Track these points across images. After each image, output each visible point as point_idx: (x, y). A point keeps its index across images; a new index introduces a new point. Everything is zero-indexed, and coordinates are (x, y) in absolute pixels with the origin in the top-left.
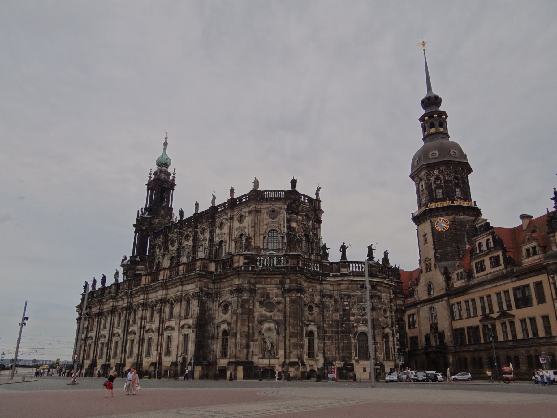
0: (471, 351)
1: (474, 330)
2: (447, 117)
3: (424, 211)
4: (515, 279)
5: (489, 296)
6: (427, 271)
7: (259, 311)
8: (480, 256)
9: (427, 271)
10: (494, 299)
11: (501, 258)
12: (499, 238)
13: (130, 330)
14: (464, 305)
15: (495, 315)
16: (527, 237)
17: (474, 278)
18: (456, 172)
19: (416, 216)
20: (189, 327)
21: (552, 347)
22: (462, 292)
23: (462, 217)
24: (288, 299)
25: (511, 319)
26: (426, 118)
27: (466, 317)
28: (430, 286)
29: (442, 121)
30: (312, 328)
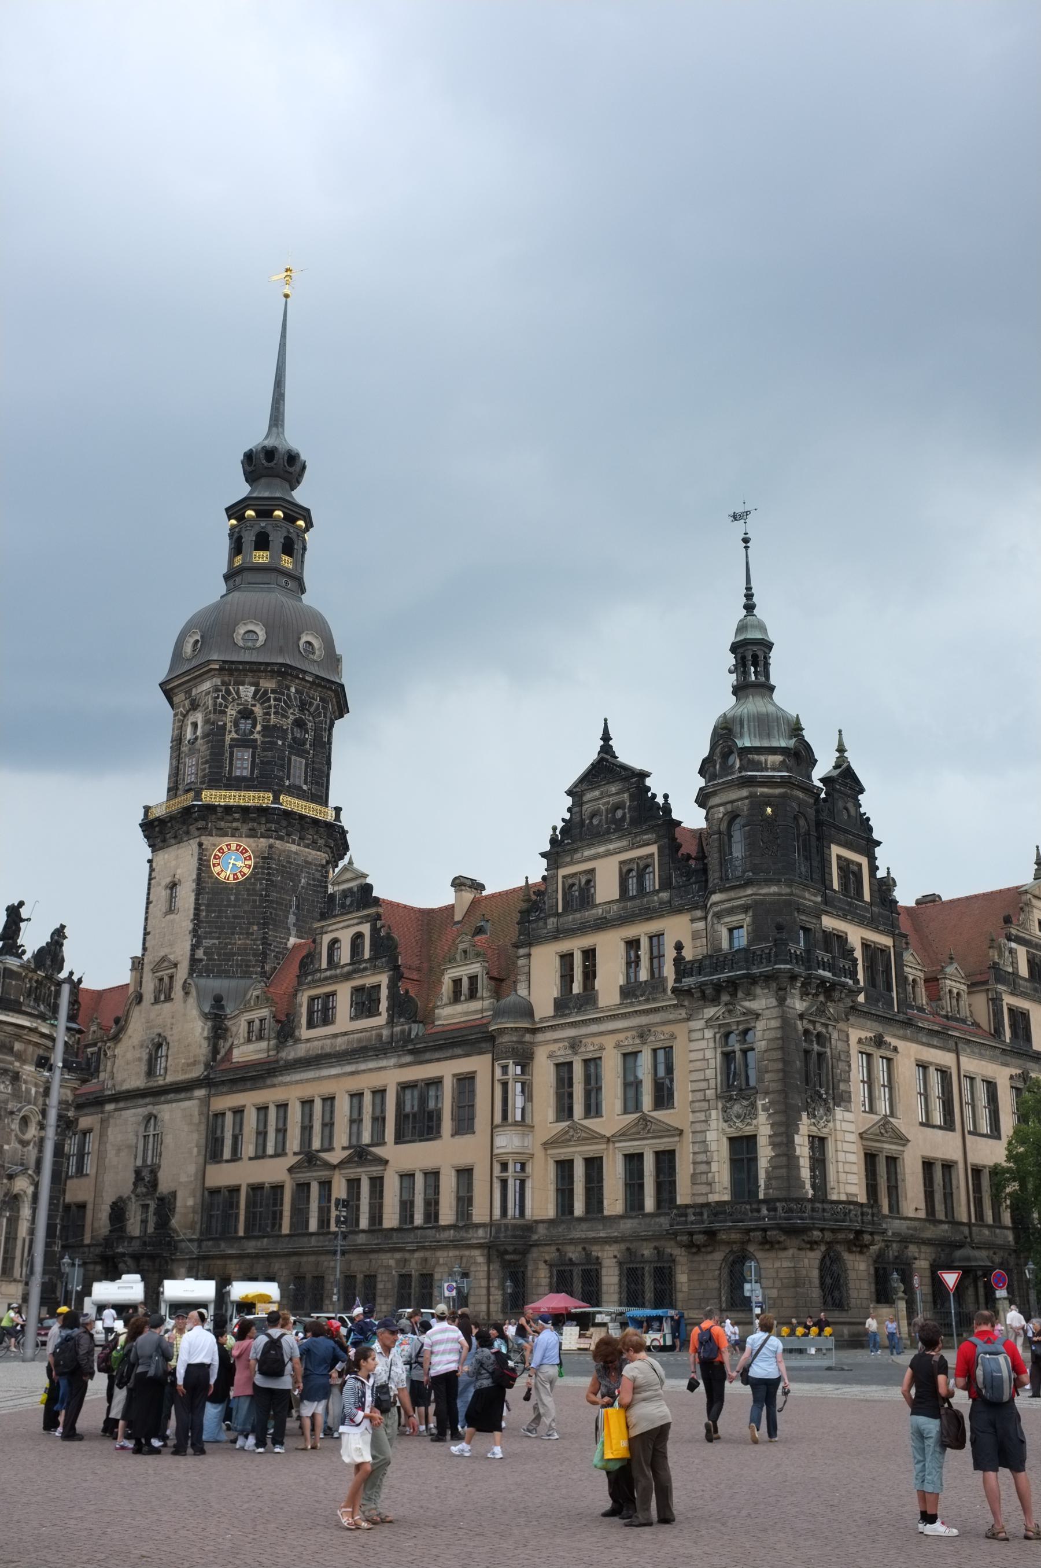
0: (249, 1256)
1: (266, 1196)
2: (309, 525)
3: (187, 810)
4: (408, 1059)
5: (329, 1100)
6: (157, 1001)
8: (326, 978)
9: (157, 1001)
10: (343, 1108)
11: (384, 992)
12: (389, 937)
14: (251, 1119)
15: (334, 1157)
16: (461, 946)
17: (298, 1041)
18: (303, 706)
19: (158, 819)
21: (467, 1253)
22: (253, 1078)
23: (294, 848)
25: (375, 1170)
26: (250, 513)
27: (252, 1154)
28: (158, 1045)
29: (294, 536)
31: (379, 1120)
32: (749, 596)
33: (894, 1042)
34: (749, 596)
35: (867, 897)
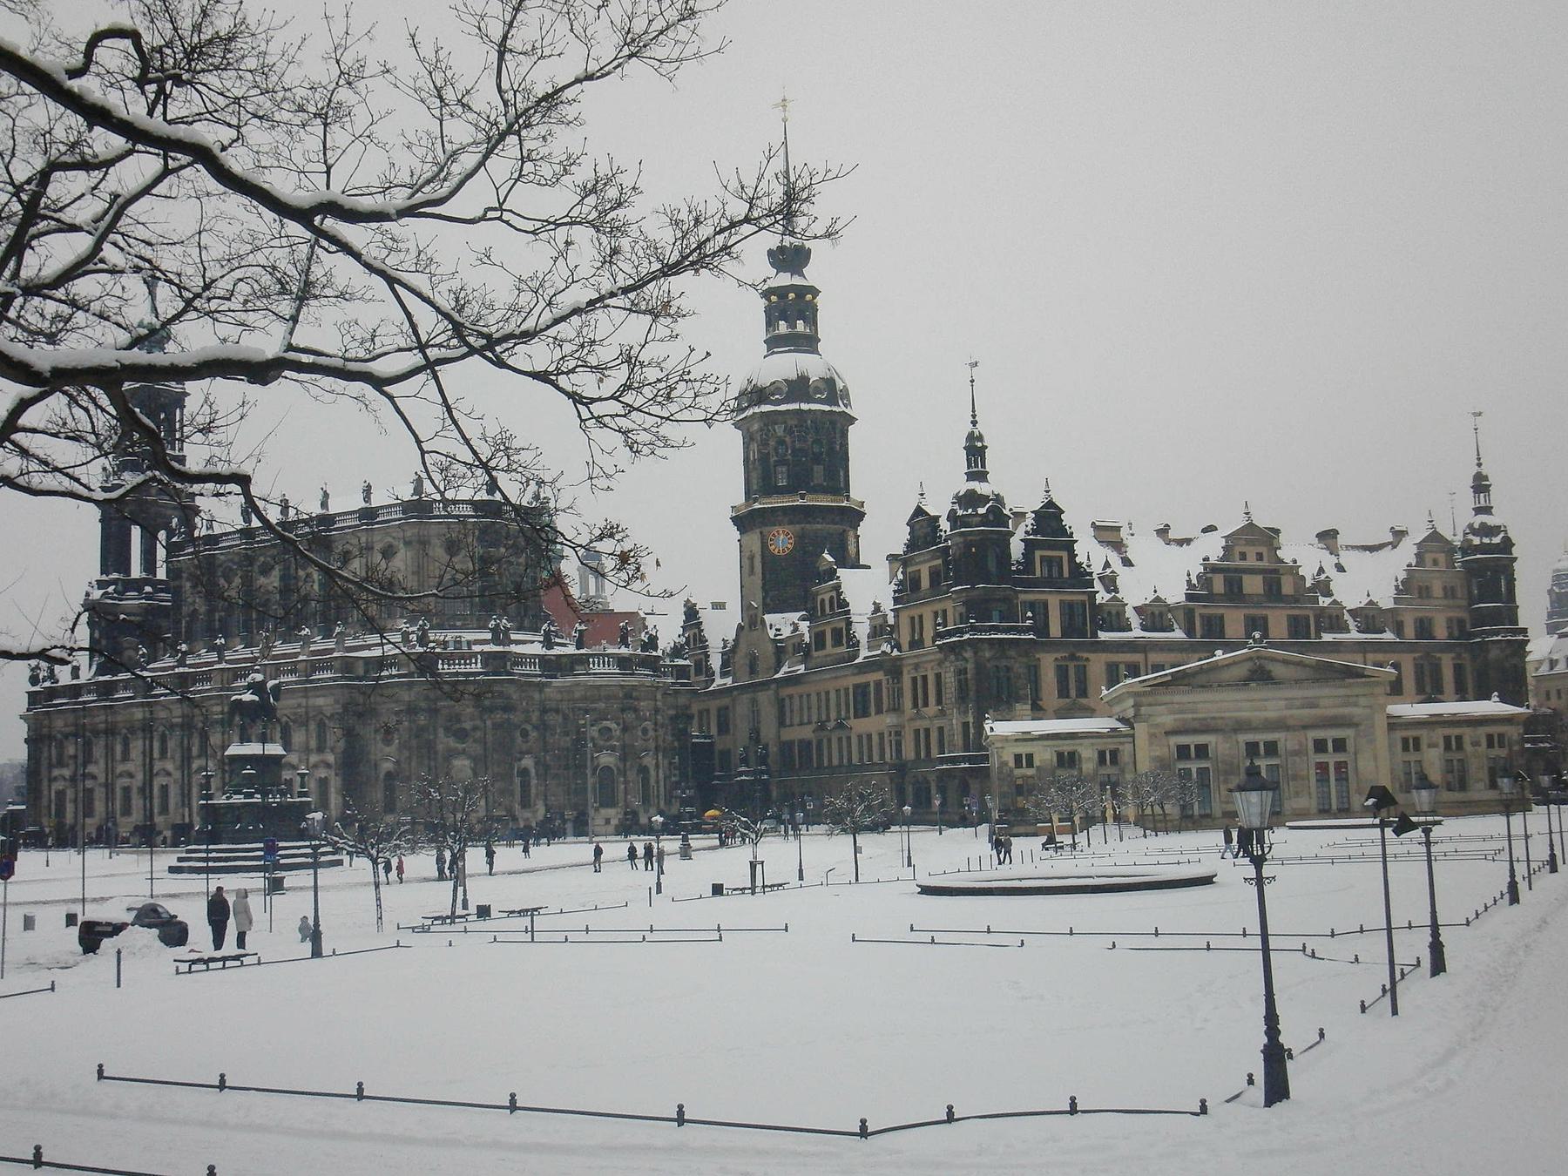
1: (805, 745)
5: (827, 693)
7: (444, 741)
10: (833, 696)
13: (195, 766)
15: (831, 725)
20: (328, 766)
24: (489, 723)
26: (774, 298)
30: (528, 762)
31: (847, 705)
32: (974, 416)
33: (1085, 655)
34: (974, 416)
35: (1066, 574)
